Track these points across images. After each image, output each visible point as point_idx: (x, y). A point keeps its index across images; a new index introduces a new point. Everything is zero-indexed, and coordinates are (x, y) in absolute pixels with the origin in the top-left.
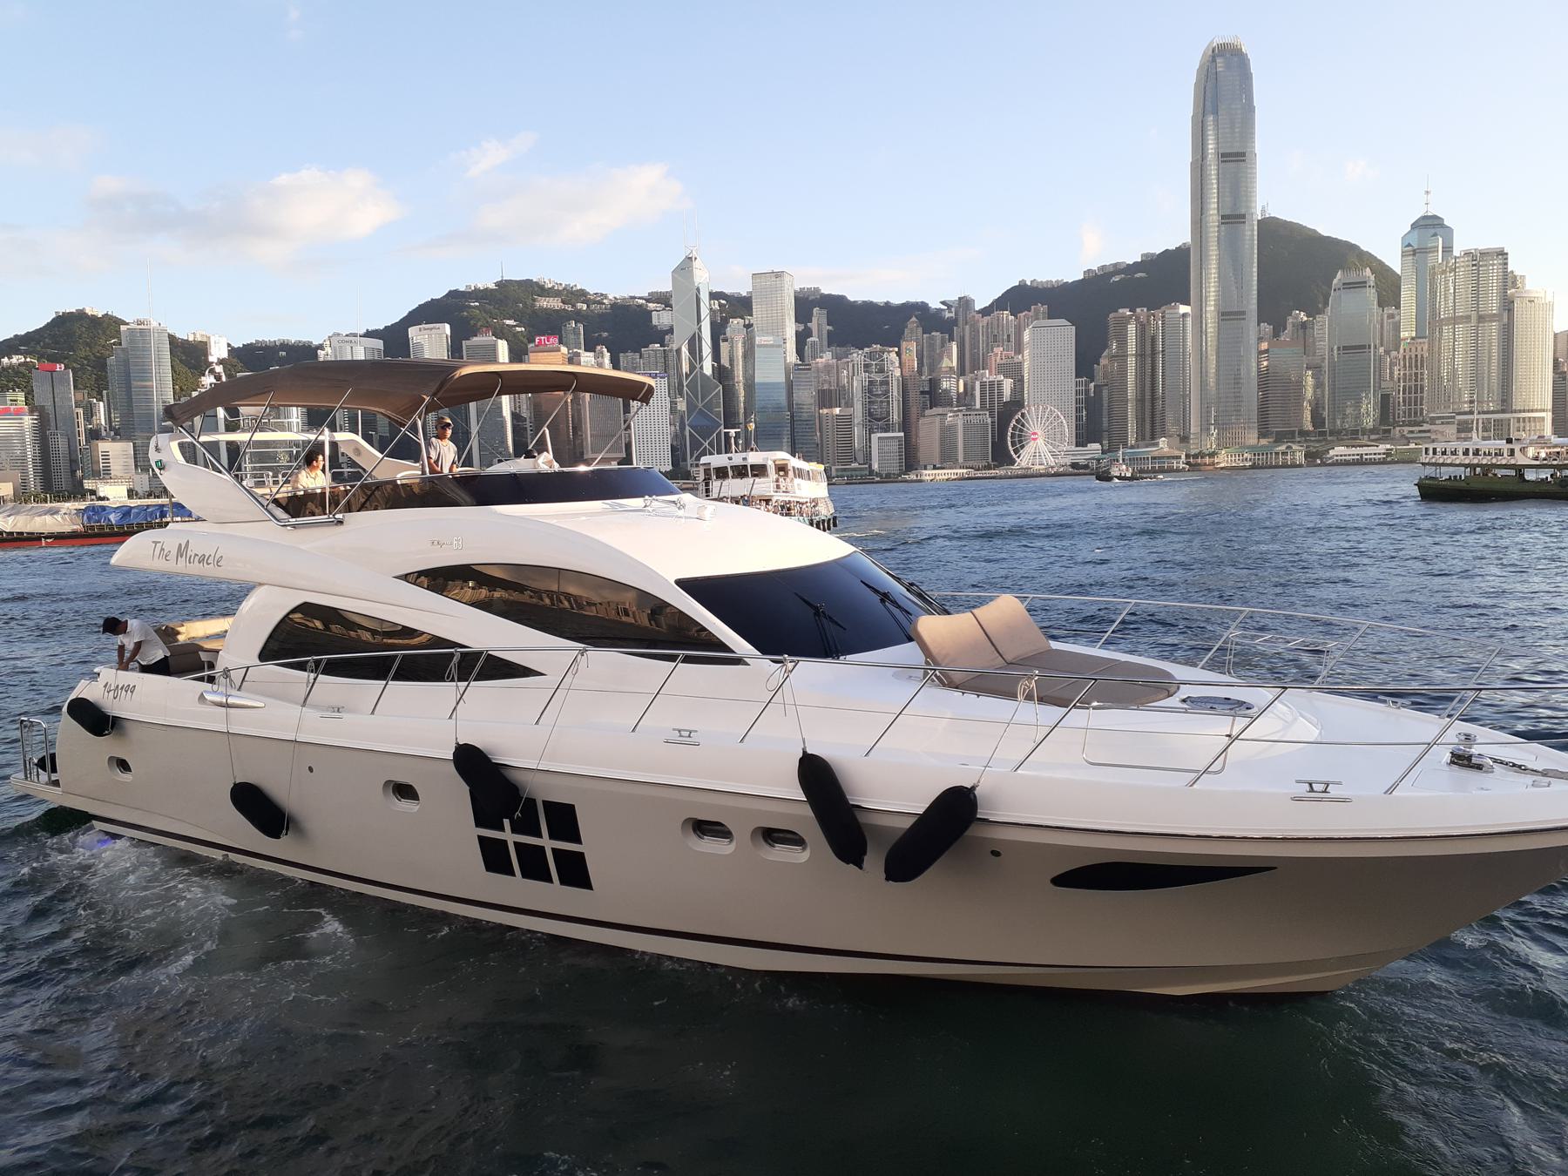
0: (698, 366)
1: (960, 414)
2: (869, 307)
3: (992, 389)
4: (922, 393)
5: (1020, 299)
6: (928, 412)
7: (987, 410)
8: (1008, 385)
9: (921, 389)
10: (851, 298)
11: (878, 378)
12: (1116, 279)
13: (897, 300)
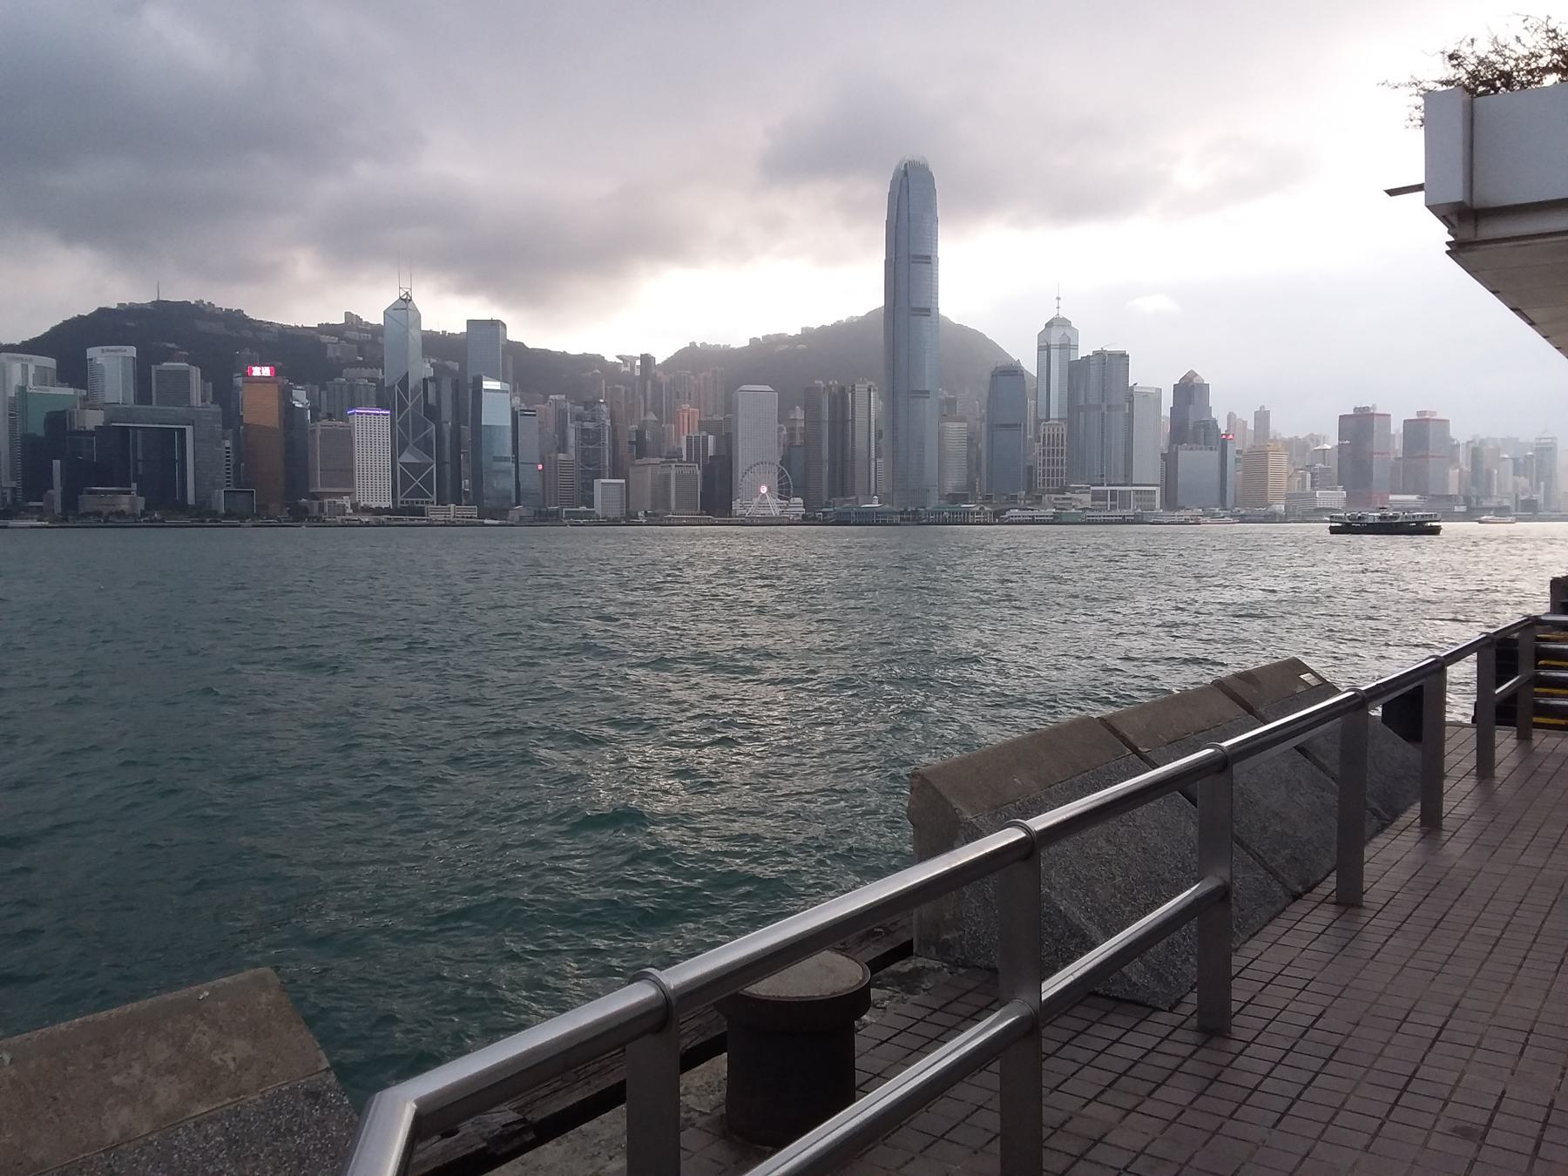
0: (410, 404)
4: (630, 442)
6: (638, 461)
7: (695, 463)
9: (628, 440)
11: (589, 425)
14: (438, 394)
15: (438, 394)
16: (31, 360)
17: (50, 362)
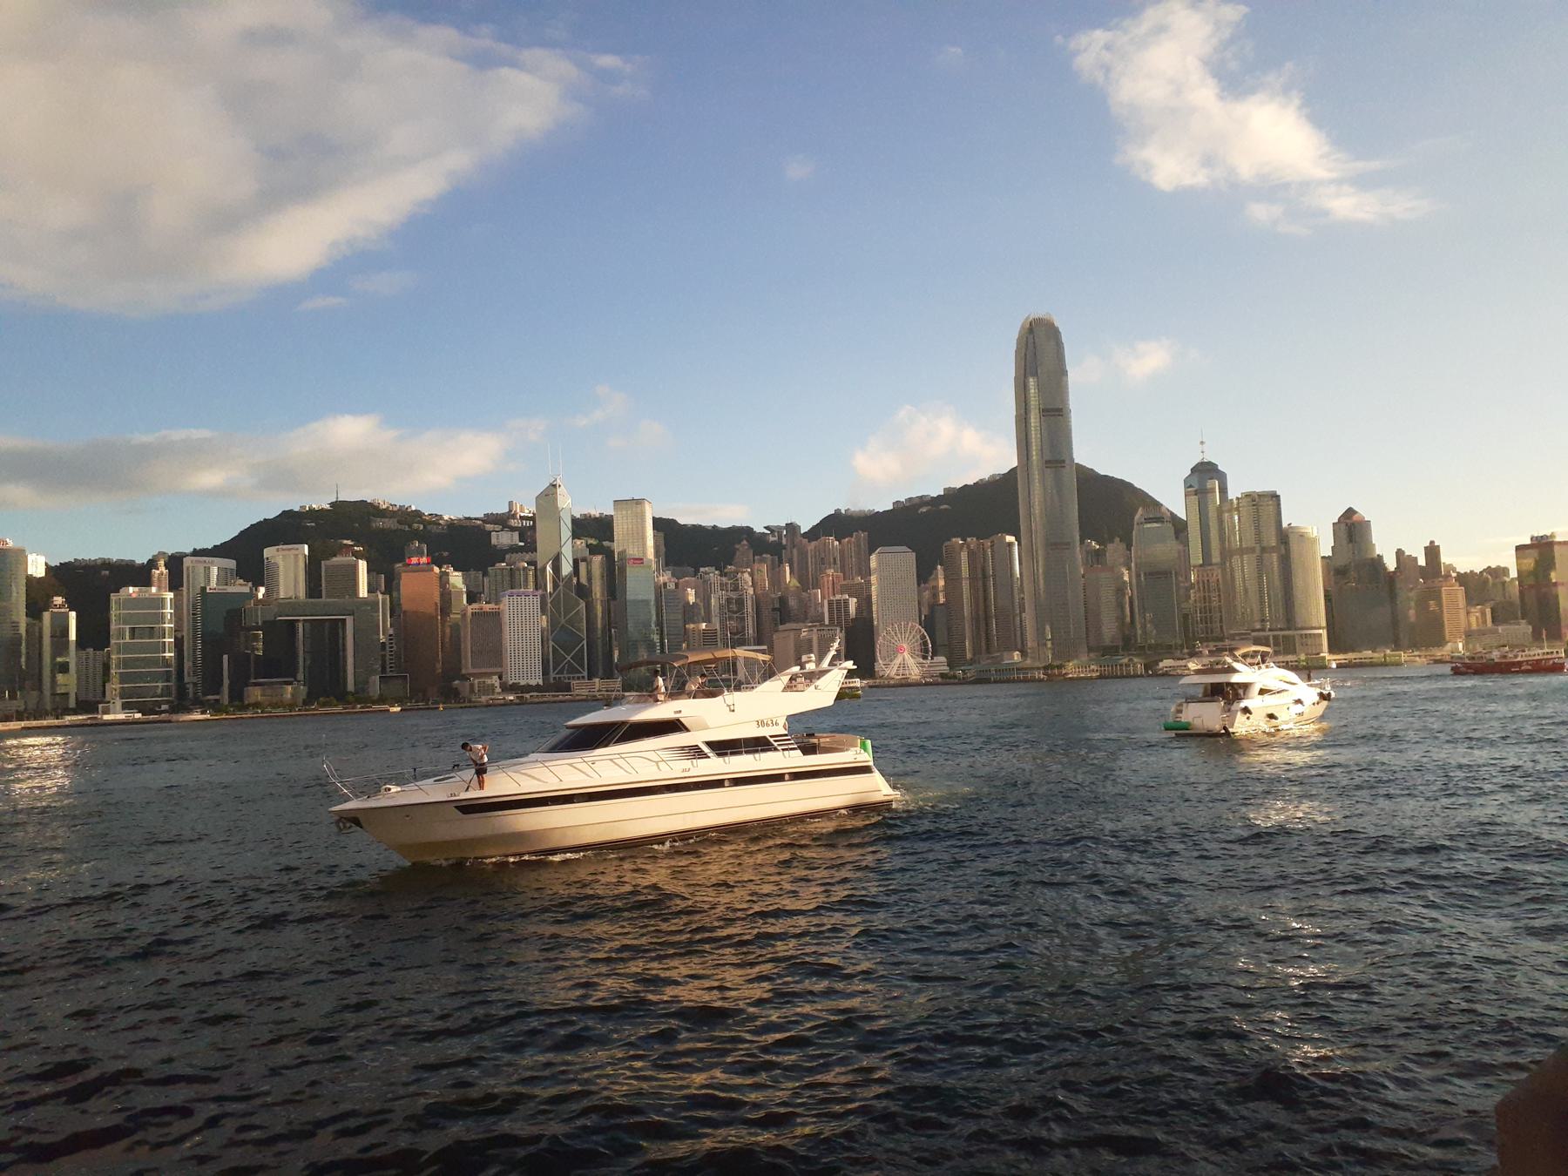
1: (815, 630)
2: (697, 529)
3: (838, 608)
4: (774, 609)
5: (836, 524)
6: (781, 627)
8: (853, 602)
10: (682, 521)
11: (734, 595)
12: (924, 510)
13: (724, 524)
14: (589, 572)
15: (589, 572)
16: (212, 563)
17: (231, 564)
